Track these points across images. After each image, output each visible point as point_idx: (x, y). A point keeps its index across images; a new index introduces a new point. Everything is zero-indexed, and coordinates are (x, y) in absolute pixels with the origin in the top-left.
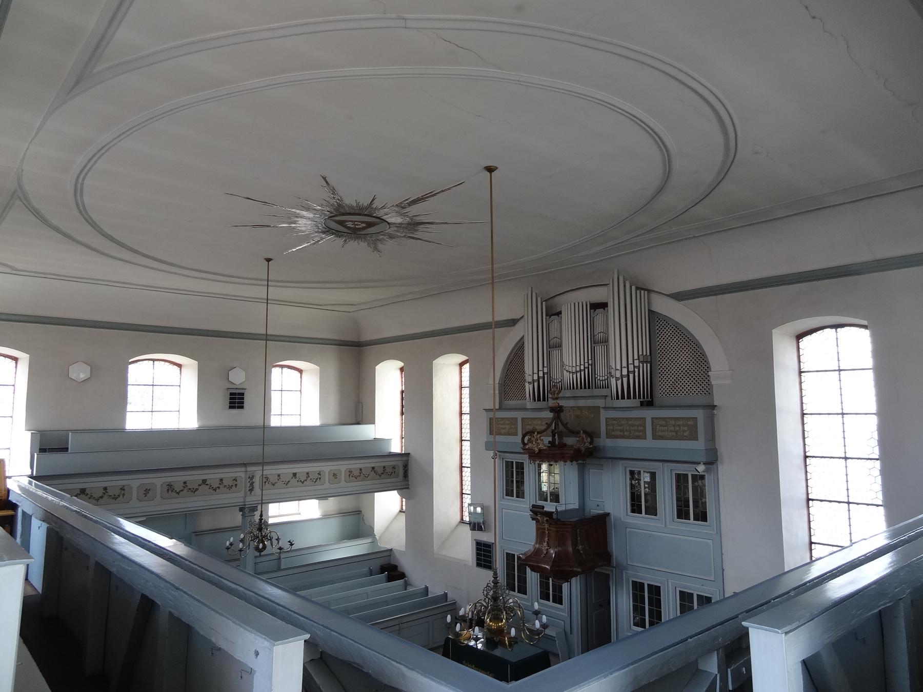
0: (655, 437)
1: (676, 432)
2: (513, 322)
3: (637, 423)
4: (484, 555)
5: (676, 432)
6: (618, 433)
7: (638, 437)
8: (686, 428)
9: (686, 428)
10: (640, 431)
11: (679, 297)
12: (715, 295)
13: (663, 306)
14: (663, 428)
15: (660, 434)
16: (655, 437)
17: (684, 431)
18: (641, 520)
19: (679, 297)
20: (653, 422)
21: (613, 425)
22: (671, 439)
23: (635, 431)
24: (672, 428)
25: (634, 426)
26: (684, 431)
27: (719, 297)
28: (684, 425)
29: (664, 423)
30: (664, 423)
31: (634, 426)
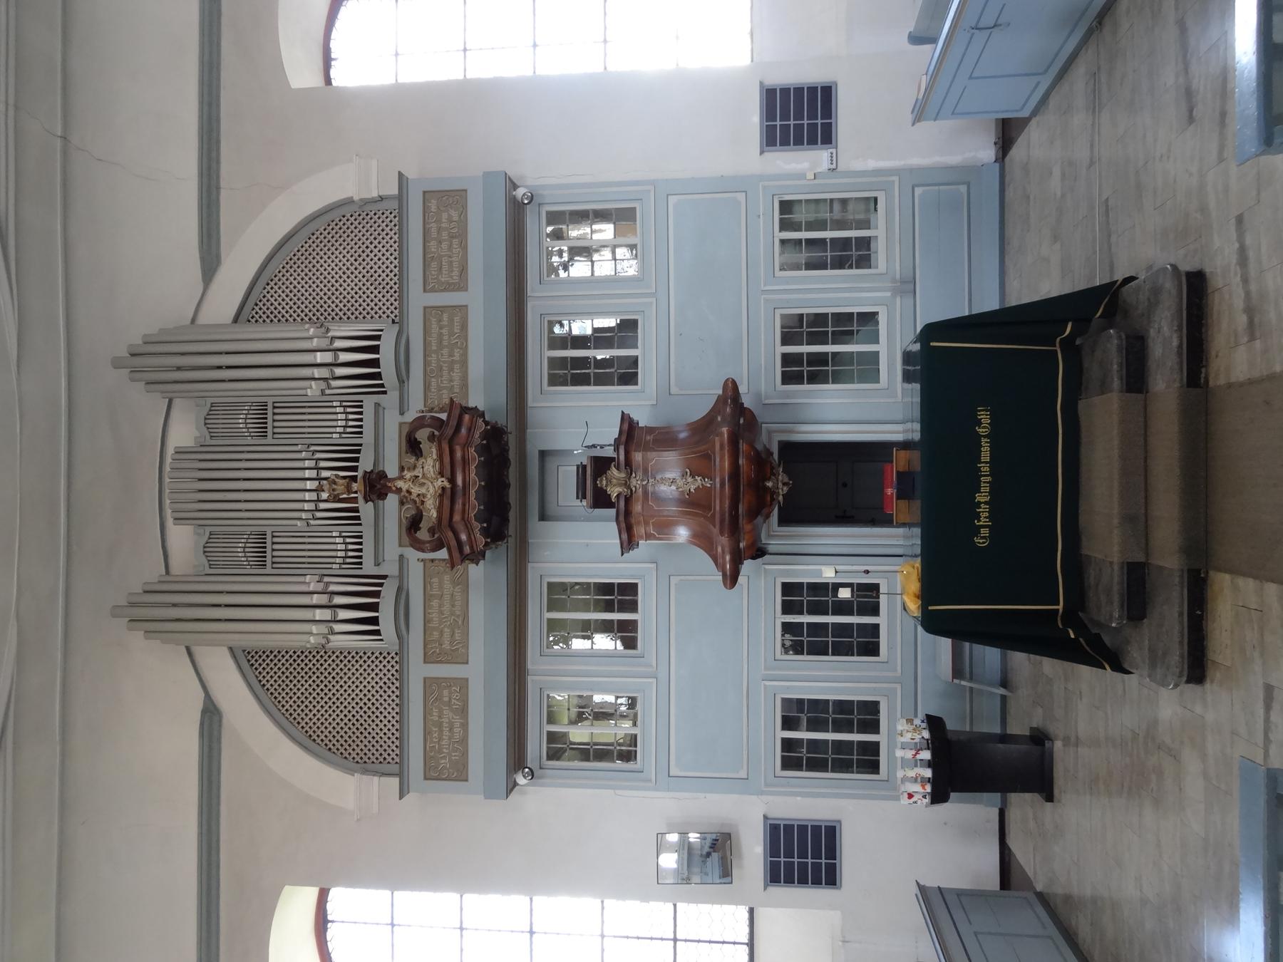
0: (461, 286)
1: (452, 237)
2: (211, 715)
3: (434, 328)
4: (805, 857)
5: (452, 237)
6: (456, 375)
7: (464, 327)
8: (445, 216)
9: (445, 216)
10: (451, 320)
11: (210, 263)
12: (218, 188)
13: (225, 299)
14: (445, 267)
15: (456, 273)
16: (461, 286)
17: (450, 220)
18: (646, 351)
19: (210, 263)
20: (433, 290)
21: (440, 389)
22: (464, 247)
23: (451, 334)
24: (445, 245)
25: (441, 335)
26: (450, 220)
27: (222, 184)
28: (439, 221)
29: (434, 264)
30: (434, 264)
31: (441, 335)
